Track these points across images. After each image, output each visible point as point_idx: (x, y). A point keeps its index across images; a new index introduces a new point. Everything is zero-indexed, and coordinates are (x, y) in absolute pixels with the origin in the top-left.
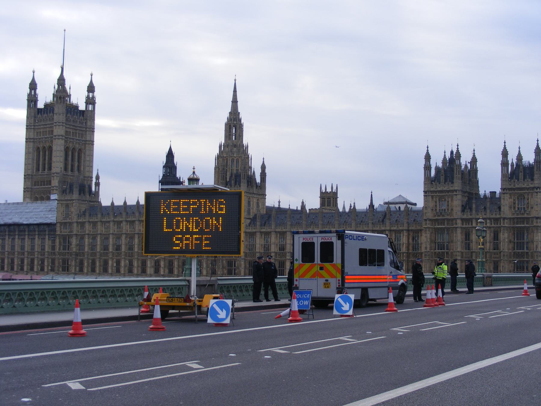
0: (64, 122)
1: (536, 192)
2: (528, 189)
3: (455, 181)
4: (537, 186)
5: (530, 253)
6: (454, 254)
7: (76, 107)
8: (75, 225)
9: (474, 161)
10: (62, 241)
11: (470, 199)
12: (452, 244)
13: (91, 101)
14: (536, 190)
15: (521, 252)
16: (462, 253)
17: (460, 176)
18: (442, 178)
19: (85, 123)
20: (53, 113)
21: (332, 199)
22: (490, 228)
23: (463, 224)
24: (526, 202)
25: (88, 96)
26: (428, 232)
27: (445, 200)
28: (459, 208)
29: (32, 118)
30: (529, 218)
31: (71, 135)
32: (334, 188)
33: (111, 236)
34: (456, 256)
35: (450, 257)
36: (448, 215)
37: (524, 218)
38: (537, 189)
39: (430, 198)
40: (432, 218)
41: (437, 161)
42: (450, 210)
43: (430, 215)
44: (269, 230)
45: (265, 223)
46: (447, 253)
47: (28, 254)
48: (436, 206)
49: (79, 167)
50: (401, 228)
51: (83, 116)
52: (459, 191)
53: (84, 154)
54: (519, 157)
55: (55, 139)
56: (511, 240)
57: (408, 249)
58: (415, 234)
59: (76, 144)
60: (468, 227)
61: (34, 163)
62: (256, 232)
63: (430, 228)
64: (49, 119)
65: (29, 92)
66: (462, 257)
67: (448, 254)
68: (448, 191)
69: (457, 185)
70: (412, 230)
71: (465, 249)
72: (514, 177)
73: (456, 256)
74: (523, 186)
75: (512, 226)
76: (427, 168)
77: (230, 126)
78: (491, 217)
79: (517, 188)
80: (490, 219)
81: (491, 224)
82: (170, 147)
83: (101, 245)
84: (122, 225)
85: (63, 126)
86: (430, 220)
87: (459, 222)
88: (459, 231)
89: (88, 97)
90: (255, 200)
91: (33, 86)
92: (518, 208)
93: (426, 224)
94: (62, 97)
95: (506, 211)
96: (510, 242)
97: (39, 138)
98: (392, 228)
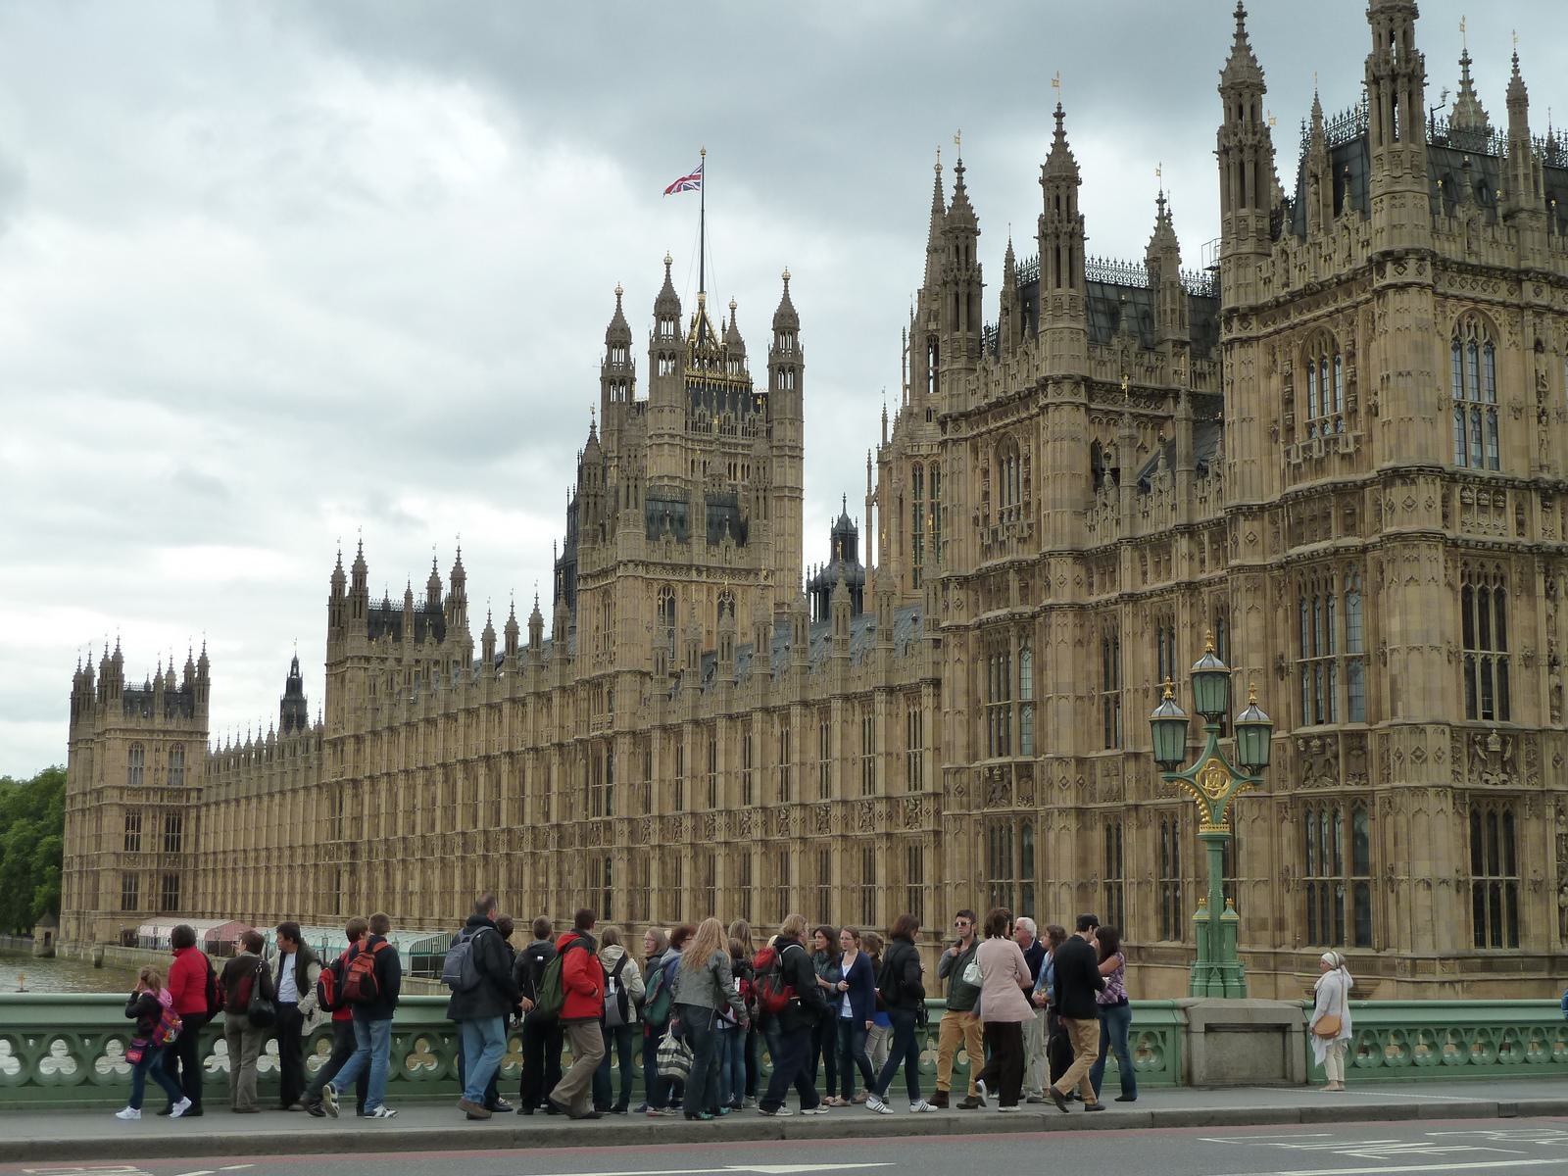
0: (674, 432)
2: (1344, 284)
4: (1380, 245)
5: (1372, 743)
13: (787, 363)
14: (1378, 283)
15: (1320, 737)
16: (1092, 762)
22: (1192, 587)
26: (954, 653)
31: (739, 474)
36: (1022, 540)
48: (986, 495)
56: (1282, 657)
60: (1107, 602)
63: (967, 628)
67: (1030, 777)
71: (1102, 743)
74: (1326, 274)
75: (1272, 559)
78: (1200, 518)
79: (1293, 295)
80: (1190, 530)
81: (1203, 561)
86: (964, 582)
87: (1063, 571)
88: (1062, 632)
89: (775, 353)
91: (618, 336)
92: (1310, 427)
96: (1281, 670)
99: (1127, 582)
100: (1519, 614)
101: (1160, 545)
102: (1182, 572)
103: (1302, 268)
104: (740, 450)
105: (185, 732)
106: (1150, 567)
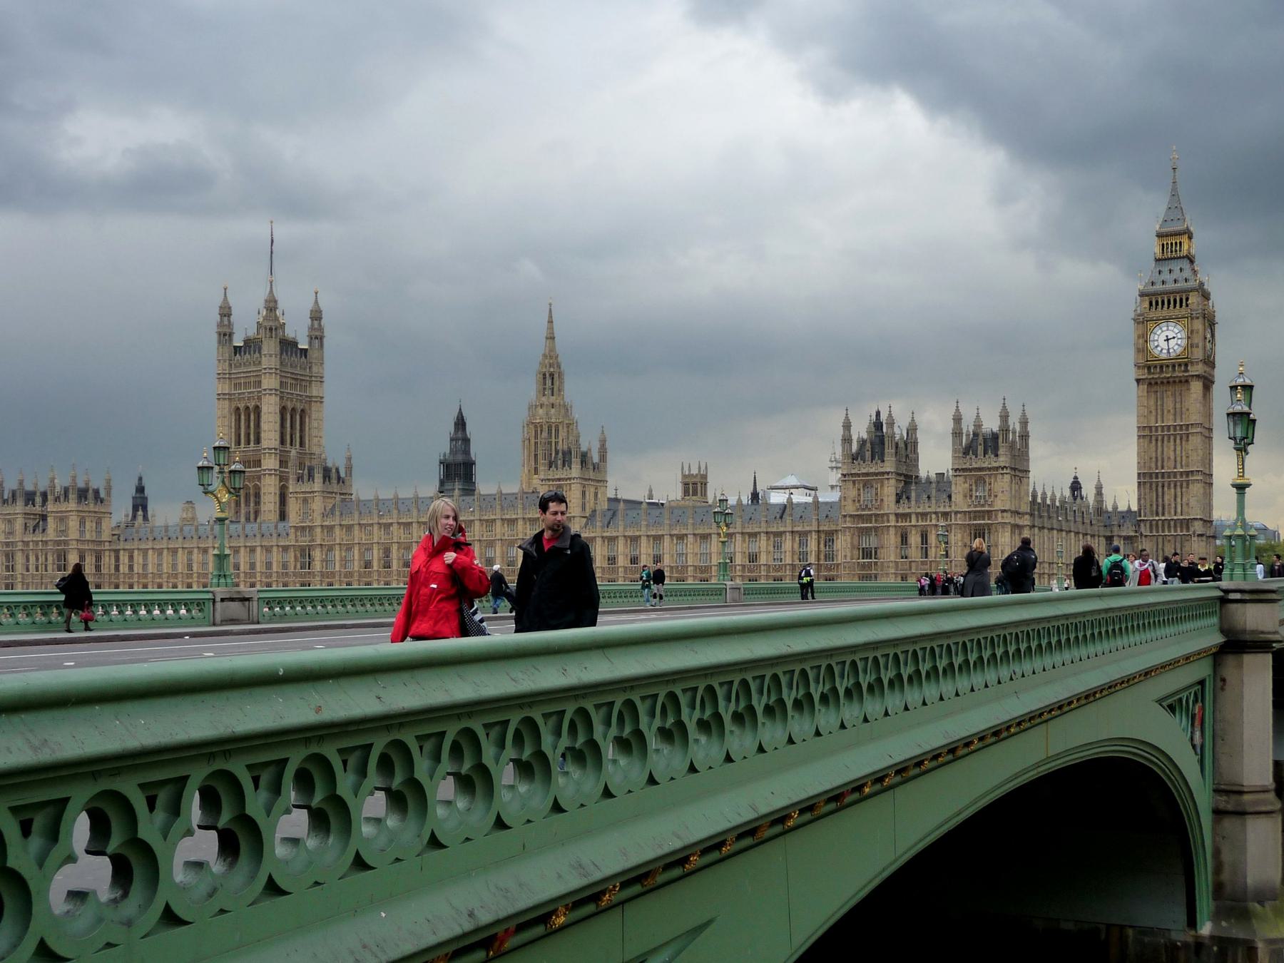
0: (278, 367)
1: (1002, 474)
2: (990, 469)
3: (885, 459)
4: (1003, 465)
6: (885, 564)
7: (294, 344)
8: (318, 530)
9: (912, 429)
10: (299, 555)
11: (906, 483)
12: (882, 551)
13: (317, 337)
17: (893, 451)
18: (868, 454)
19: (310, 368)
20: (260, 352)
21: (699, 485)
23: (897, 522)
24: (987, 488)
25: (312, 325)
26: (848, 534)
27: (872, 487)
28: (893, 498)
29: (225, 362)
30: (991, 511)
32: (703, 468)
33: (375, 547)
34: (888, 567)
35: (879, 570)
36: (876, 508)
37: (983, 511)
38: (1003, 469)
39: (851, 486)
40: (856, 513)
41: (861, 430)
42: (879, 500)
43: (851, 509)
44: (615, 534)
45: (609, 523)
46: (876, 563)
47: (245, 577)
48: (859, 495)
49: (301, 438)
50: (808, 528)
51: (306, 357)
52: (892, 473)
53: (309, 417)
54: (978, 425)
55: (265, 394)
57: (819, 559)
58: (829, 537)
59: (296, 401)
61: (231, 432)
62: (595, 537)
64: (254, 362)
65: (219, 320)
66: (897, 569)
68: (876, 474)
69: (889, 465)
70: (823, 531)
72: (971, 452)
73: (888, 567)
75: (967, 523)
76: (847, 440)
77: (544, 375)
80: (936, 513)
82: (460, 409)
83: (360, 560)
84: (391, 528)
85: (276, 374)
86: (851, 516)
87: (892, 518)
88: (892, 531)
89: (312, 328)
90: (592, 490)
91: (226, 312)
93: (845, 522)
94: (274, 328)
95: (960, 502)
97: (238, 393)
98: (795, 529)
99: (914, 522)
100: (1014, 538)
101: (924, 515)
102: (934, 522)
103: (976, 463)
104: (299, 377)
105: (102, 512)
106: (920, 518)
